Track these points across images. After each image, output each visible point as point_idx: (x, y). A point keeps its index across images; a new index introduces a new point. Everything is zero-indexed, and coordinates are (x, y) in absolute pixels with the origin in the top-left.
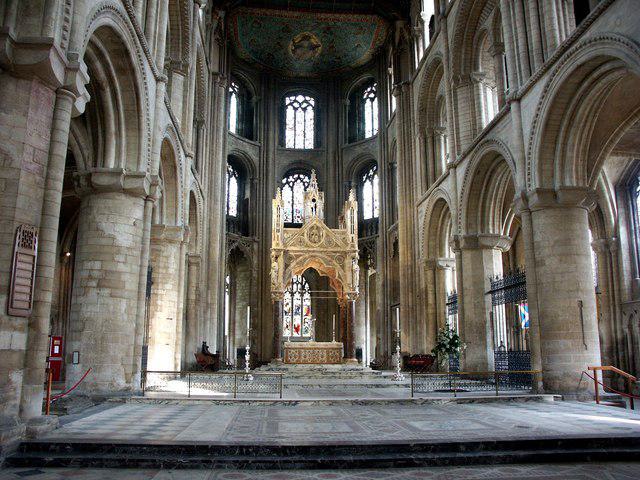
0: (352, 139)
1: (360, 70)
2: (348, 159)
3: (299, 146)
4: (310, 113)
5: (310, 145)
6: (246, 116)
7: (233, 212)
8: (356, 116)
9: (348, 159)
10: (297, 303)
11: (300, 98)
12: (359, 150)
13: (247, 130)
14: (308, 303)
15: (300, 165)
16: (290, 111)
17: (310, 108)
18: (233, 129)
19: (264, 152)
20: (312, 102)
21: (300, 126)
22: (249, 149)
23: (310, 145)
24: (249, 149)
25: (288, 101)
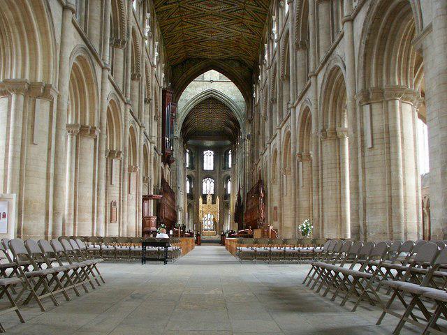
0: (225, 168)
1: (227, 146)
2: (223, 175)
3: (208, 169)
4: (212, 157)
5: (212, 169)
6: (191, 160)
7: (188, 192)
8: (226, 160)
9: (223, 175)
10: (209, 217)
11: (209, 151)
12: (226, 173)
13: (192, 167)
14: (212, 217)
15: (208, 174)
16: (205, 156)
17: (212, 156)
18: (187, 166)
19: (197, 173)
20: (212, 152)
21: (209, 161)
22: (192, 173)
23: (212, 169)
24: (192, 173)
25: (205, 152)
